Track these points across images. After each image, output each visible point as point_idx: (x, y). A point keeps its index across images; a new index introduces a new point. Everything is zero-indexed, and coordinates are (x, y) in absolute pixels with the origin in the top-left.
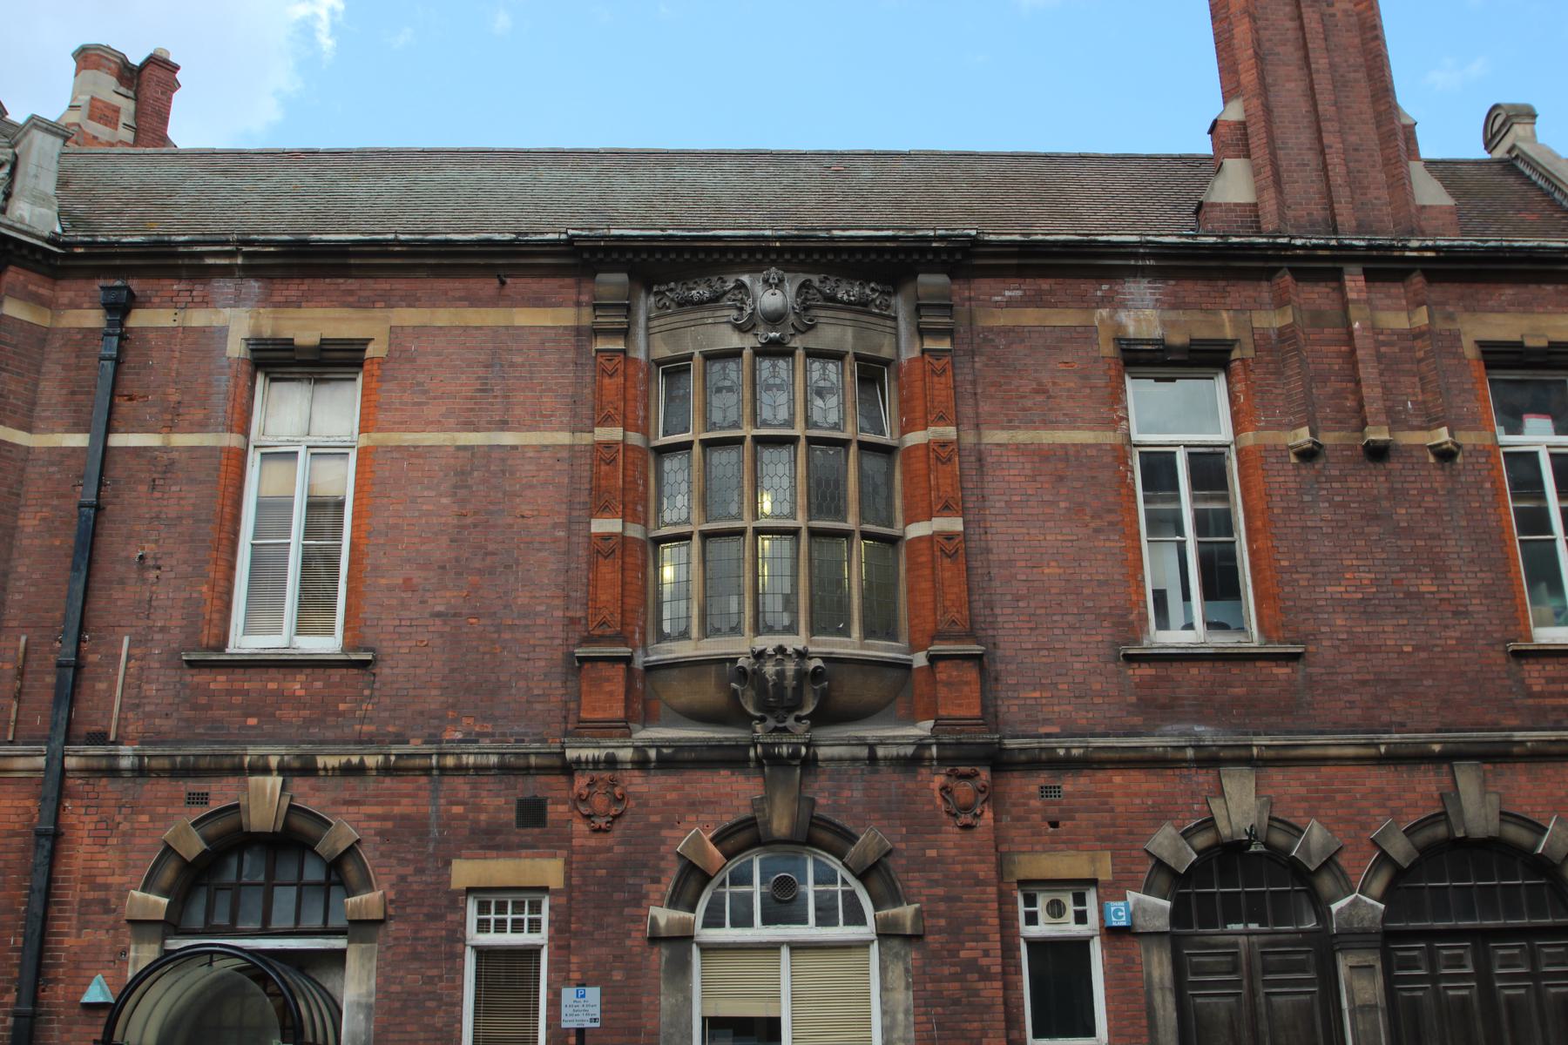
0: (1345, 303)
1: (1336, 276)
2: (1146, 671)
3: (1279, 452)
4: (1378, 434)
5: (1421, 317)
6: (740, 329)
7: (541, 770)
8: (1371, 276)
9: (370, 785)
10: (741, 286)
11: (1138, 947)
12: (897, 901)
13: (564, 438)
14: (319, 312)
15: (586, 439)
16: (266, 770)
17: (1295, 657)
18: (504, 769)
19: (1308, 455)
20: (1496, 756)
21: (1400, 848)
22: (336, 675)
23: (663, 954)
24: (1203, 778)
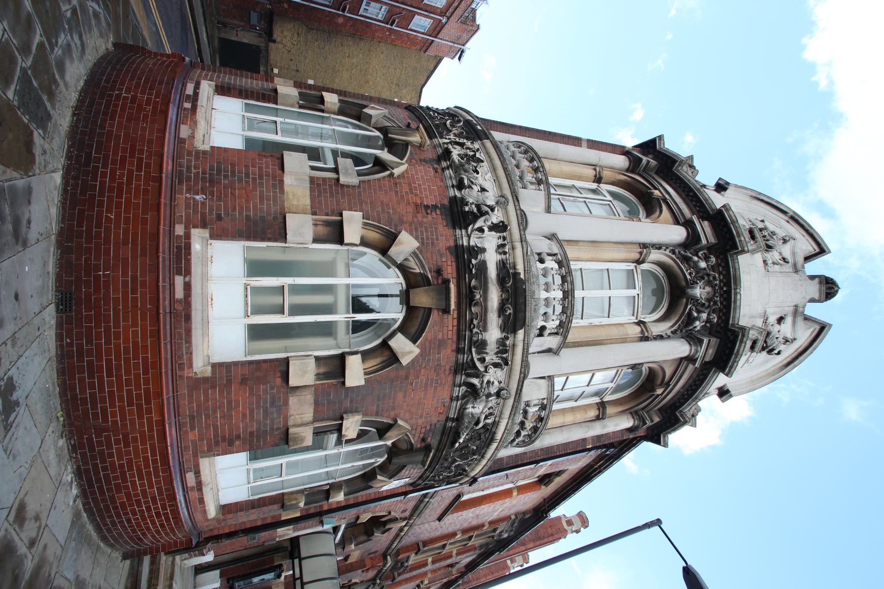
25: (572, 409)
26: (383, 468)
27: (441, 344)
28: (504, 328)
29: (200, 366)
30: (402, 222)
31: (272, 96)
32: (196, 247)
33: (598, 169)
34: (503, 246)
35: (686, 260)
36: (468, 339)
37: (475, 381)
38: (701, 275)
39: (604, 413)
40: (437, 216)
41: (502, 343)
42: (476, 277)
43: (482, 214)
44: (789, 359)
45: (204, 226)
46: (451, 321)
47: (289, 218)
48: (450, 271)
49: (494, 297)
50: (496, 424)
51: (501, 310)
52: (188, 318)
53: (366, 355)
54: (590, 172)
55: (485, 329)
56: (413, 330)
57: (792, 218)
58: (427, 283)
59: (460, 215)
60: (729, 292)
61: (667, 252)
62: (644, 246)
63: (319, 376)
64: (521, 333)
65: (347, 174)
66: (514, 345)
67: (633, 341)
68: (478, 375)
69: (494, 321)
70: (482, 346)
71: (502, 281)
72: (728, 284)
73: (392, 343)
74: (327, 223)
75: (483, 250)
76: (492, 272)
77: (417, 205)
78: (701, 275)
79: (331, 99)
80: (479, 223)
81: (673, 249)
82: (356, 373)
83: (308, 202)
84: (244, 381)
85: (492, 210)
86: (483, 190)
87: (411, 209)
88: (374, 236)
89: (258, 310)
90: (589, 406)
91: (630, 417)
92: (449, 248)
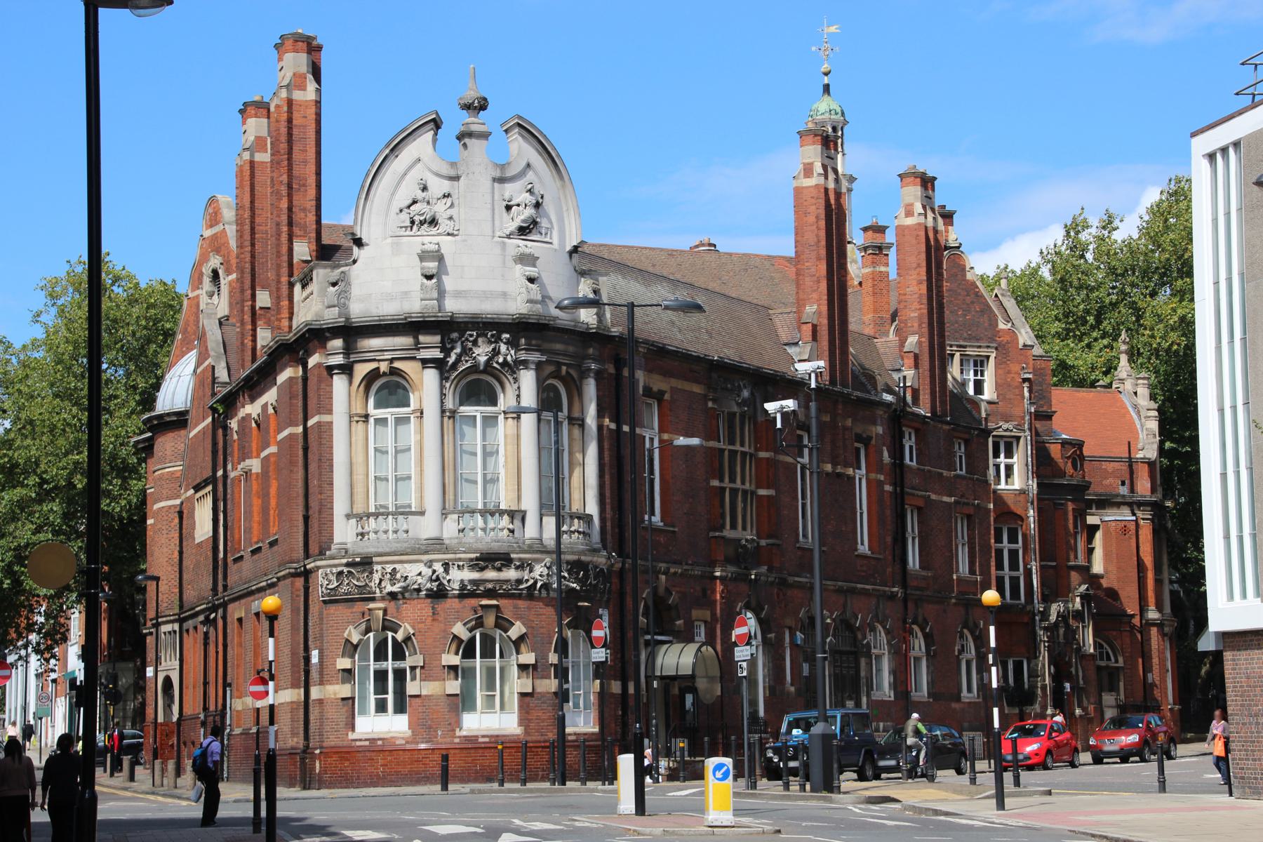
4: (839, 469)
5: (849, 422)
6: (738, 404)
19: (827, 474)
27: (516, 607)
30: (445, 631)
32: (464, 733)
36: (513, 592)
37: (539, 585)
39: (578, 419)
41: (517, 568)
43: (438, 579)
44: (550, 162)
45: (454, 730)
47: (448, 692)
48: (474, 602)
49: (491, 574)
51: (499, 570)
55: (507, 581)
57: (392, 150)
58: (481, 617)
59: (439, 594)
60: (484, 323)
61: (448, 385)
62: (443, 412)
64: (513, 556)
66: (520, 559)
67: (518, 427)
68: (536, 583)
70: (519, 581)
71: (482, 569)
75: (462, 581)
76: (475, 575)
78: (466, 351)
80: (445, 582)
81: (443, 378)
82: (528, 658)
83: (437, 683)
84: (527, 713)
85: (434, 572)
86: (420, 574)
87: (436, 624)
88: (454, 647)
89: (492, 706)
90: (569, 431)
91: (585, 381)
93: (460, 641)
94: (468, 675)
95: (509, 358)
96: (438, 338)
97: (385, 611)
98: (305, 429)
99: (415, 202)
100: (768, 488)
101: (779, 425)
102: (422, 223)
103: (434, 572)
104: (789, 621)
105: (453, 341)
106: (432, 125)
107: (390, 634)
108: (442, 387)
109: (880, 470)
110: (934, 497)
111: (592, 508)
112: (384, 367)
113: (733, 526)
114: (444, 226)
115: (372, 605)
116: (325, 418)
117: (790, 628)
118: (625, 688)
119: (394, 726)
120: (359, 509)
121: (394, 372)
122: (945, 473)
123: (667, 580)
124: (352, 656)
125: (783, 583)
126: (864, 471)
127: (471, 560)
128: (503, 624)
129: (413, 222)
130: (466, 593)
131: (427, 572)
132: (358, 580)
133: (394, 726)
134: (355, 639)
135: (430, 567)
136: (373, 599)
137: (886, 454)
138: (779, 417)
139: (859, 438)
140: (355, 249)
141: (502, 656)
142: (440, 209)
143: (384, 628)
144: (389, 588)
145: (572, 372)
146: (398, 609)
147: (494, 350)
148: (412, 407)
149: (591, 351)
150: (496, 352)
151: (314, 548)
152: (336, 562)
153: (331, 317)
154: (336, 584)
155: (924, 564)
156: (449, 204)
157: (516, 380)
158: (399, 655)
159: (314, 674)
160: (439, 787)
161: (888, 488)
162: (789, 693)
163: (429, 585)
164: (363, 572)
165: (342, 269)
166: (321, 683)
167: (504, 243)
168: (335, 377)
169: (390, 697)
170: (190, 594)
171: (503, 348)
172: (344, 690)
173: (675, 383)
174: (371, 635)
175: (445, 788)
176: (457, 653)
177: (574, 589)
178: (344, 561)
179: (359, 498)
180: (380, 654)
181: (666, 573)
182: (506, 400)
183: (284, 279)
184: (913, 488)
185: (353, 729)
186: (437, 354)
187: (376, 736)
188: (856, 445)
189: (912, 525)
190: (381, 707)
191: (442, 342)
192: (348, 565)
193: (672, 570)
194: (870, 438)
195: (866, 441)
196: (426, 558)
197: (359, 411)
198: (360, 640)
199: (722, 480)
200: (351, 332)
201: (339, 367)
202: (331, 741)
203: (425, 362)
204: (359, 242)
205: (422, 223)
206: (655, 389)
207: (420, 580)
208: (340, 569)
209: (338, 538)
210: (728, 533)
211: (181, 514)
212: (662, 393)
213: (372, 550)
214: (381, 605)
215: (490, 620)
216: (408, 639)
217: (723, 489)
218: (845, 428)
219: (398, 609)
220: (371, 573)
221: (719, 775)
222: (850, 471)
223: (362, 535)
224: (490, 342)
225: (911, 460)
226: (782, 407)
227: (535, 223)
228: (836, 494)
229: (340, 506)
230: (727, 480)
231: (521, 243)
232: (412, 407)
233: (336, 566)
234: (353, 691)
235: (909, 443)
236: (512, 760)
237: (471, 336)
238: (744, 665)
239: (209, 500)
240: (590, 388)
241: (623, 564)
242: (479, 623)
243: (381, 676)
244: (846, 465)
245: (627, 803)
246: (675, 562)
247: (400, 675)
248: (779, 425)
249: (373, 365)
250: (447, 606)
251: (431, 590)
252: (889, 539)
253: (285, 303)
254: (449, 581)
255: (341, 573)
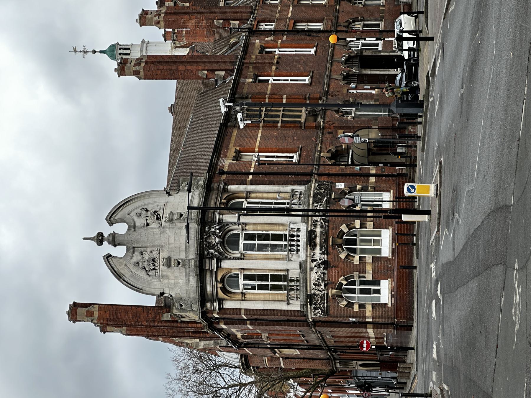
0: (250, 63)
1: (244, 63)
2: (313, 84)
3: (275, 71)
5: (254, 57)
7: (323, 131)
8: (245, 59)
9: (323, 147)
10: (234, 112)
11: (358, 87)
12: (350, 100)
13: (260, 131)
14: (228, 154)
15: (261, 128)
16: (320, 155)
17: (313, 72)
18: (323, 134)
19: (277, 68)
20: (332, 57)
21: (346, 66)
22: (303, 150)
23: (356, 119)
24: (332, 80)
25: (263, 198)
26: (346, 194)
27: (333, 228)
28: (315, 231)
29: (391, 228)
30: (343, 262)
31: (374, 306)
32: (391, 254)
33: (243, 298)
34: (313, 255)
35: (220, 253)
38: (213, 247)
39: (247, 194)
40: (332, 264)
42: (323, 246)
43: (319, 265)
46: (331, 234)
48: (330, 248)
49: (318, 240)
50: (313, 203)
51: (316, 236)
52: (392, 239)
53: (354, 228)
54: (247, 296)
55: (321, 231)
56: (342, 233)
58: (337, 245)
59: (326, 264)
60: (200, 239)
63: (366, 224)
64: (309, 229)
65: (357, 275)
66: (311, 226)
69: (318, 234)
70: (322, 227)
71: (315, 245)
72: (200, 242)
73: (348, 230)
74: (362, 261)
75: (320, 254)
76: (318, 248)
77: (338, 267)
78: (213, 247)
79: (356, 308)
82: (357, 223)
85: (315, 266)
86: (316, 273)
88: (351, 258)
89: (379, 240)
92: (330, 254)
93: (348, 254)
94: (363, 251)
95: (217, 227)
96: (207, 261)
97: (333, 289)
98: (248, 320)
99: (144, 268)
100: (283, 98)
101: (250, 122)
102: (154, 265)
103: (315, 266)
104: (345, 91)
105: (209, 253)
106: (109, 259)
107: (344, 287)
108: (230, 259)
109: (276, 41)
110: (289, 15)
111: (289, 188)
112: (220, 285)
113: (300, 117)
114: (155, 254)
115: (330, 295)
116: (243, 312)
117: (348, 90)
118: (373, 175)
119: (385, 286)
120: (285, 298)
121: (222, 280)
122: (279, 9)
123: (324, 152)
124: (353, 304)
125: (327, 93)
126: (276, 50)
127: (310, 249)
128: (342, 233)
129: (154, 269)
130: (325, 251)
131: (315, 271)
132: (318, 300)
133: (385, 286)
134: (345, 303)
135: (313, 269)
136: (327, 294)
137: (269, 38)
138: (245, 122)
139: (261, 51)
140: (165, 295)
141: (356, 236)
142: (147, 257)
143: (341, 289)
144: (322, 287)
145: (224, 197)
146: (332, 283)
147: (213, 235)
148: (239, 273)
149: (215, 187)
150: (214, 233)
151: (303, 318)
152: (309, 310)
153: (196, 307)
154: (319, 310)
155: (320, 21)
156: (145, 253)
157: (228, 225)
158: (354, 283)
159: (361, 320)
160: (414, 271)
161: (285, 37)
162: (378, 92)
163: (322, 269)
164: (314, 298)
165: (174, 301)
166: (365, 317)
167: (163, 227)
168: (224, 307)
169: (373, 287)
170: (322, 356)
171: (213, 230)
172: (369, 308)
173: (231, 145)
174: (343, 295)
175: (415, 268)
176: (354, 257)
177: (326, 200)
178: (309, 306)
179: (280, 298)
180: (353, 291)
181: (320, 152)
182: (237, 229)
183: (179, 325)
184: (285, 26)
185: (386, 304)
186: (214, 261)
187: (390, 295)
188: (264, 52)
189: (302, 26)
190: (377, 292)
191: (209, 258)
192: (311, 305)
193: (319, 149)
194: (261, 46)
195: (263, 48)
196: (308, 270)
197: (240, 297)
198: (346, 300)
199: (278, 122)
200: (203, 298)
201: (219, 305)
202: (391, 313)
203: (218, 266)
204: (162, 294)
205: (154, 265)
206: (234, 154)
207: (319, 273)
208: (313, 308)
209: (299, 309)
210: (303, 120)
211: (287, 358)
212: (236, 151)
213: (305, 294)
214: (330, 291)
215: (339, 241)
216: (346, 279)
217: (282, 121)
218: (256, 58)
219: (332, 283)
220: (315, 294)
221: (412, 190)
222: (276, 57)
223: (297, 298)
224: (210, 236)
225: (272, 25)
226: (241, 120)
227: (155, 212)
228: (286, 65)
229: (283, 306)
230: (278, 119)
231: (164, 220)
232: (239, 273)
233: (311, 310)
234: (369, 304)
235: (264, 26)
236: (404, 239)
237: (206, 244)
238: (362, 139)
239: (281, 350)
240: (233, 188)
241: (315, 174)
242: (340, 246)
243: (362, 291)
244: (273, 58)
245: (425, 218)
246: (316, 147)
247: (363, 283)
248: (250, 122)
249: (219, 290)
250: (331, 260)
251: (324, 269)
252: (308, 38)
253: (190, 325)
254: (320, 260)
255: (314, 307)
